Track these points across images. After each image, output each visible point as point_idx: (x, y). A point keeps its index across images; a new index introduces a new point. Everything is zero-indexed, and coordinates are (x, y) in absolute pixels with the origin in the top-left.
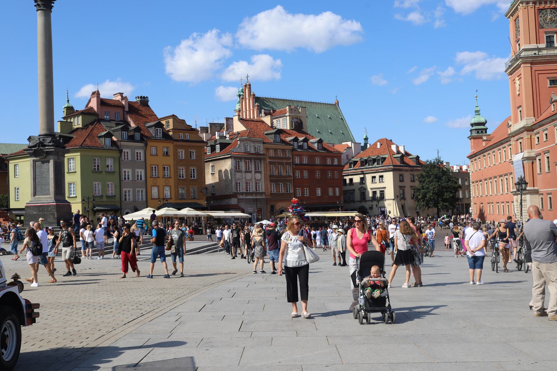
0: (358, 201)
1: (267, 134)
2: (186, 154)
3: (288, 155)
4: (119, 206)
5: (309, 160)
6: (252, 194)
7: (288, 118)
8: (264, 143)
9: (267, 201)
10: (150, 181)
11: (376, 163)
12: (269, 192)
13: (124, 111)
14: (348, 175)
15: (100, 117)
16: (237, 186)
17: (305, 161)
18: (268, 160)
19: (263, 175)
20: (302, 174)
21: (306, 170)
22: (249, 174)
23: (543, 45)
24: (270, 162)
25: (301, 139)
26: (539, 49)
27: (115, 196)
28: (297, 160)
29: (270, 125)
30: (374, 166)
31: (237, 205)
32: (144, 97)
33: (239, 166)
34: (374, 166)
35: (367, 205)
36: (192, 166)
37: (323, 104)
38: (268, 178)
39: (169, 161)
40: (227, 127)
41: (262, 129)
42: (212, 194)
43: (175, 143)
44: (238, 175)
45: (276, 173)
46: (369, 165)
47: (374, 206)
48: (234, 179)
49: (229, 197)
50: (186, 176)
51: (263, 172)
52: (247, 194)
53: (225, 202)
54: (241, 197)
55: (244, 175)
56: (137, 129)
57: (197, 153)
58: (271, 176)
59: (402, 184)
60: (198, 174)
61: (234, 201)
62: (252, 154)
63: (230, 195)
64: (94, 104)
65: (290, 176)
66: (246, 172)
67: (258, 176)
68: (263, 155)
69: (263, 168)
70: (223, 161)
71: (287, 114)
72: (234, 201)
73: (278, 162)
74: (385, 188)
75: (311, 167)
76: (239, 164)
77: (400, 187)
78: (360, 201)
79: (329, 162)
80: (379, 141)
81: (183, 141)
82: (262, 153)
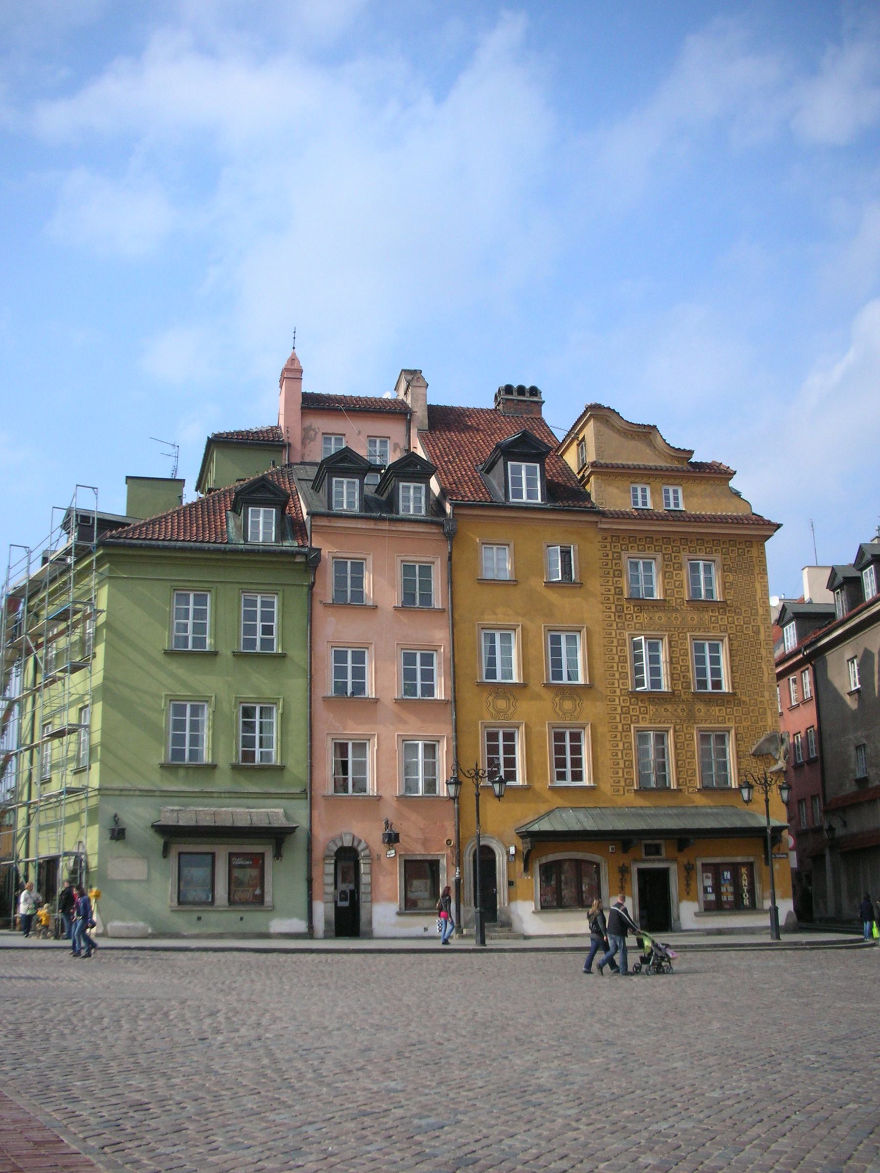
32: (521, 390)
50: (673, 678)
57: (726, 569)
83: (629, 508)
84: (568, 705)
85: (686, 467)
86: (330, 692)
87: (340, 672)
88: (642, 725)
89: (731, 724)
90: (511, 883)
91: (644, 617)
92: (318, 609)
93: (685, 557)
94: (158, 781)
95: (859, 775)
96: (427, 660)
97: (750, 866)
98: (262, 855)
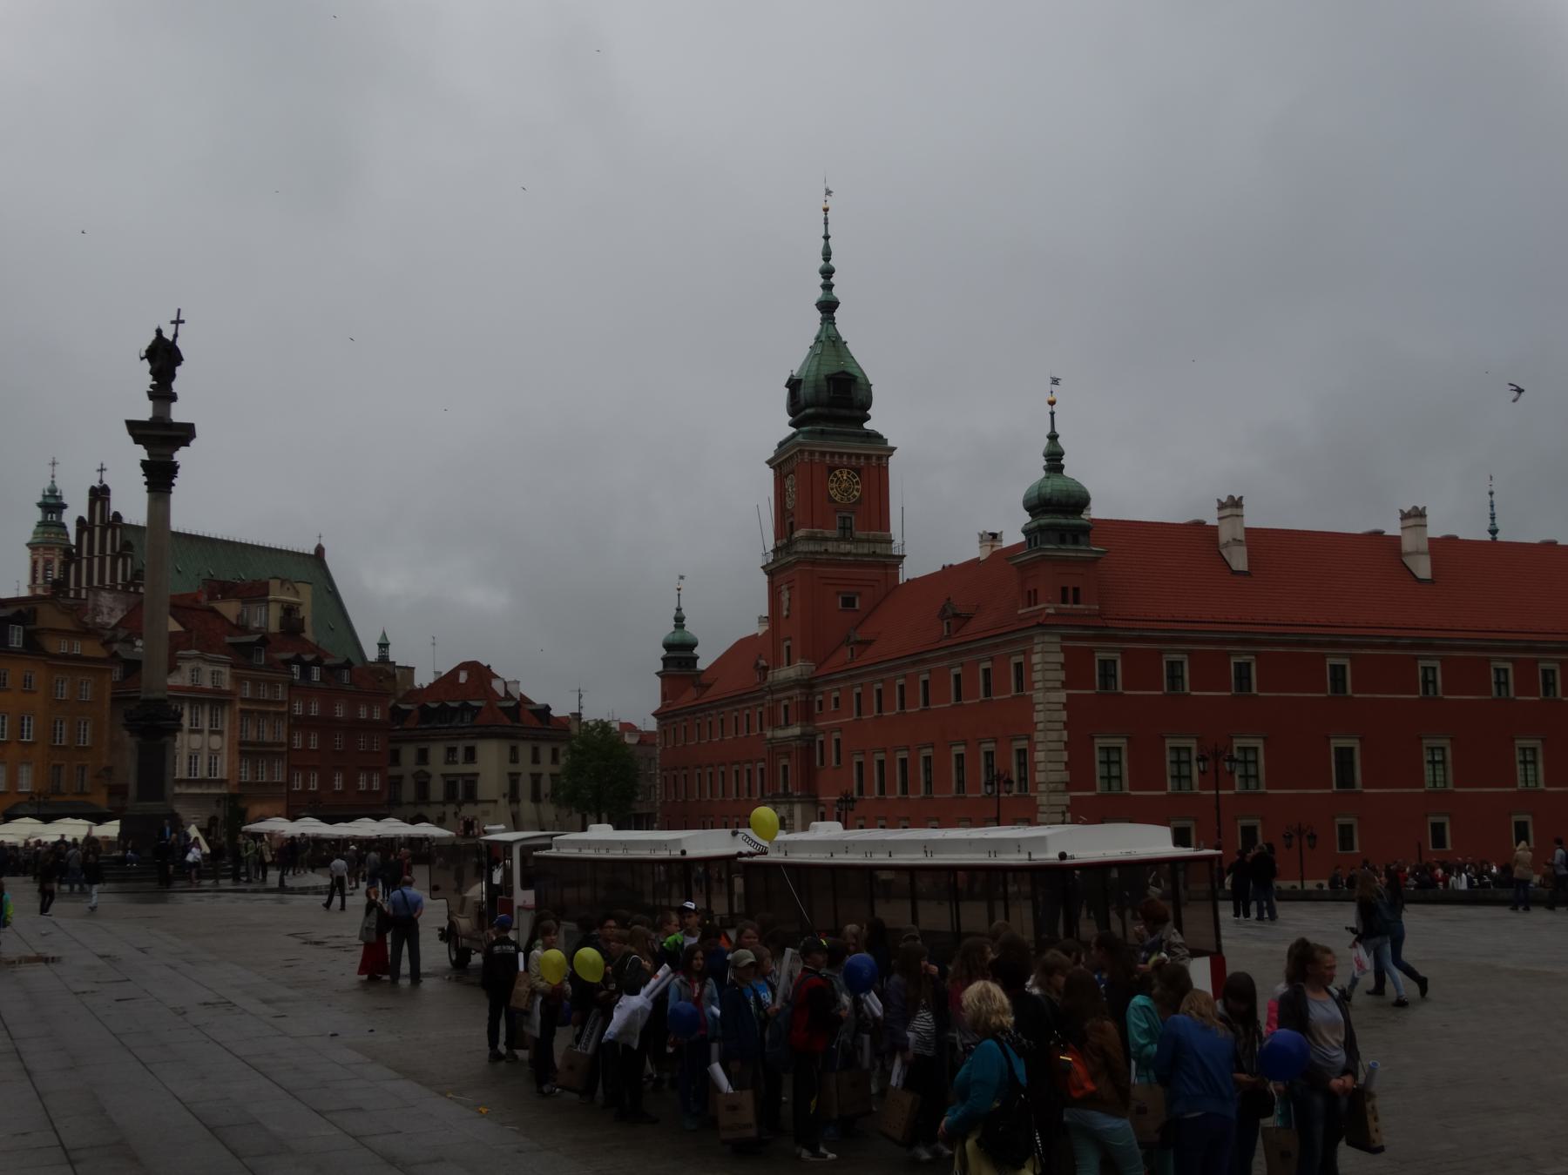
1: (231, 644)
3: (281, 694)
8: (232, 666)
9: (232, 798)
17: (315, 710)
18: (239, 706)
20: (306, 741)
22: (197, 737)
23: (835, 533)
24: (242, 711)
25: (308, 658)
26: (826, 539)
28: (298, 709)
45: (252, 735)
52: (189, 783)
58: (241, 744)
59: (514, 768)
65: (281, 745)
67: (216, 741)
69: (226, 724)
74: (477, 775)
77: (511, 774)
78: (415, 804)
79: (363, 713)
80: (465, 666)
81: (66, 657)
82: (226, 687)
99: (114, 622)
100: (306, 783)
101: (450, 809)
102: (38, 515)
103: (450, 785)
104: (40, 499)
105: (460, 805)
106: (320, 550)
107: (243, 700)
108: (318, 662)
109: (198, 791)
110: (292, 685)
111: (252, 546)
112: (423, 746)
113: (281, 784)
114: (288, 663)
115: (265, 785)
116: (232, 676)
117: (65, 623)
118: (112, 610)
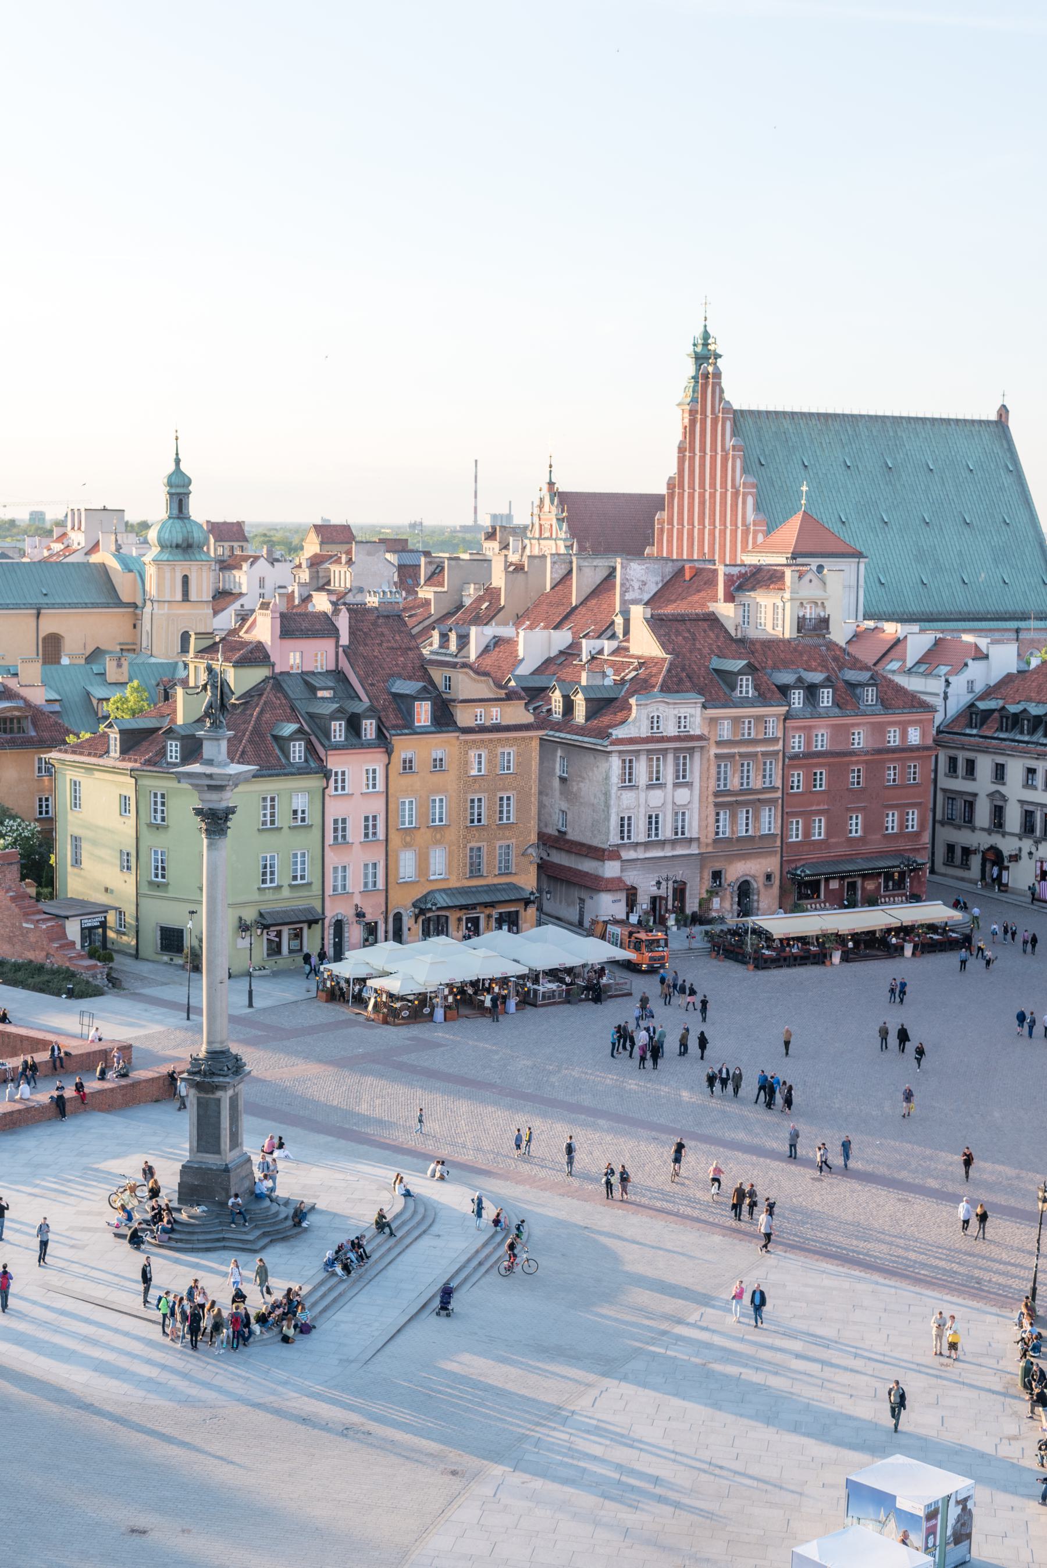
0: (983, 829)
2: (489, 761)
3: (774, 729)
4: (320, 910)
5: (833, 739)
6: (662, 843)
7: (788, 605)
8: (704, 707)
10: (395, 839)
11: (1040, 732)
12: (712, 836)
13: (337, 646)
14: (963, 749)
15: (277, 670)
16: (622, 826)
17: (822, 741)
18: (714, 750)
19: (696, 792)
21: (820, 765)
24: (717, 756)
25: (817, 677)
27: (310, 884)
28: (797, 744)
29: (733, 633)
30: (1034, 739)
31: (619, 880)
33: (630, 774)
34: (1034, 739)
35: (1007, 846)
36: (505, 789)
37: (957, 421)
38: (711, 799)
39: (450, 779)
40: (622, 585)
41: (706, 651)
42: (559, 831)
43: (463, 737)
44: (628, 797)
45: (734, 783)
46: (1022, 733)
47: (1024, 854)
48: (613, 811)
49: (599, 854)
50: (489, 817)
51: (697, 785)
52: (647, 845)
53: (587, 866)
54: (631, 854)
55: (642, 795)
56: (372, 712)
57: (518, 755)
58: (717, 794)
60: (518, 810)
61: (611, 869)
62: (669, 739)
63: (604, 850)
64: (263, 630)
65: (774, 789)
66: (650, 787)
67: (683, 795)
68: (700, 738)
70: (590, 758)
71: (787, 595)
72: (611, 869)
73: (741, 755)
75: (838, 758)
76: (630, 768)
78: (989, 831)
79: (893, 738)
81: (483, 729)
82: (698, 732)
83: (471, 723)
84: (438, 836)
85: (504, 696)
86: (332, 842)
87: (336, 830)
88: (473, 844)
89: (514, 840)
90: (409, 929)
91: (477, 786)
92: (327, 798)
93: (500, 750)
94: (256, 896)
95: (560, 827)
96: (375, 818)
97: (517, 912)
98: (301, 929)
99: (646, 597)
100: (807, 833)
101: (1027, 844)
102: (690, 368)
103: (1028, 815)
104: (690, 349)
105: (1037, 842)
106: (1003, 411)
107: (719, 743)
108: (828, 683)
109: (660, 854)
110: (787, 717)
111: (909, 419)
112: (1000, 760)
113: (774, 835)
114: (784, 690)
115: (751, 838)
116: (704, 719)
117: (483, 689)
118: (644, 583)
